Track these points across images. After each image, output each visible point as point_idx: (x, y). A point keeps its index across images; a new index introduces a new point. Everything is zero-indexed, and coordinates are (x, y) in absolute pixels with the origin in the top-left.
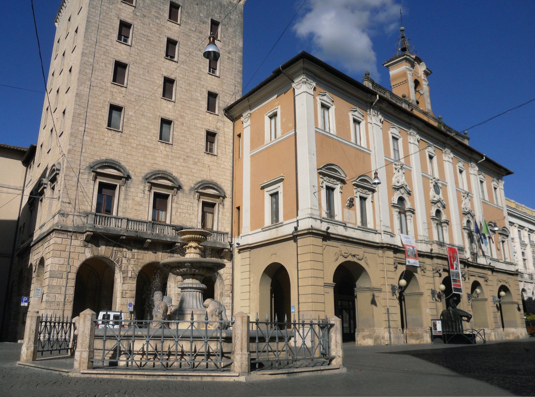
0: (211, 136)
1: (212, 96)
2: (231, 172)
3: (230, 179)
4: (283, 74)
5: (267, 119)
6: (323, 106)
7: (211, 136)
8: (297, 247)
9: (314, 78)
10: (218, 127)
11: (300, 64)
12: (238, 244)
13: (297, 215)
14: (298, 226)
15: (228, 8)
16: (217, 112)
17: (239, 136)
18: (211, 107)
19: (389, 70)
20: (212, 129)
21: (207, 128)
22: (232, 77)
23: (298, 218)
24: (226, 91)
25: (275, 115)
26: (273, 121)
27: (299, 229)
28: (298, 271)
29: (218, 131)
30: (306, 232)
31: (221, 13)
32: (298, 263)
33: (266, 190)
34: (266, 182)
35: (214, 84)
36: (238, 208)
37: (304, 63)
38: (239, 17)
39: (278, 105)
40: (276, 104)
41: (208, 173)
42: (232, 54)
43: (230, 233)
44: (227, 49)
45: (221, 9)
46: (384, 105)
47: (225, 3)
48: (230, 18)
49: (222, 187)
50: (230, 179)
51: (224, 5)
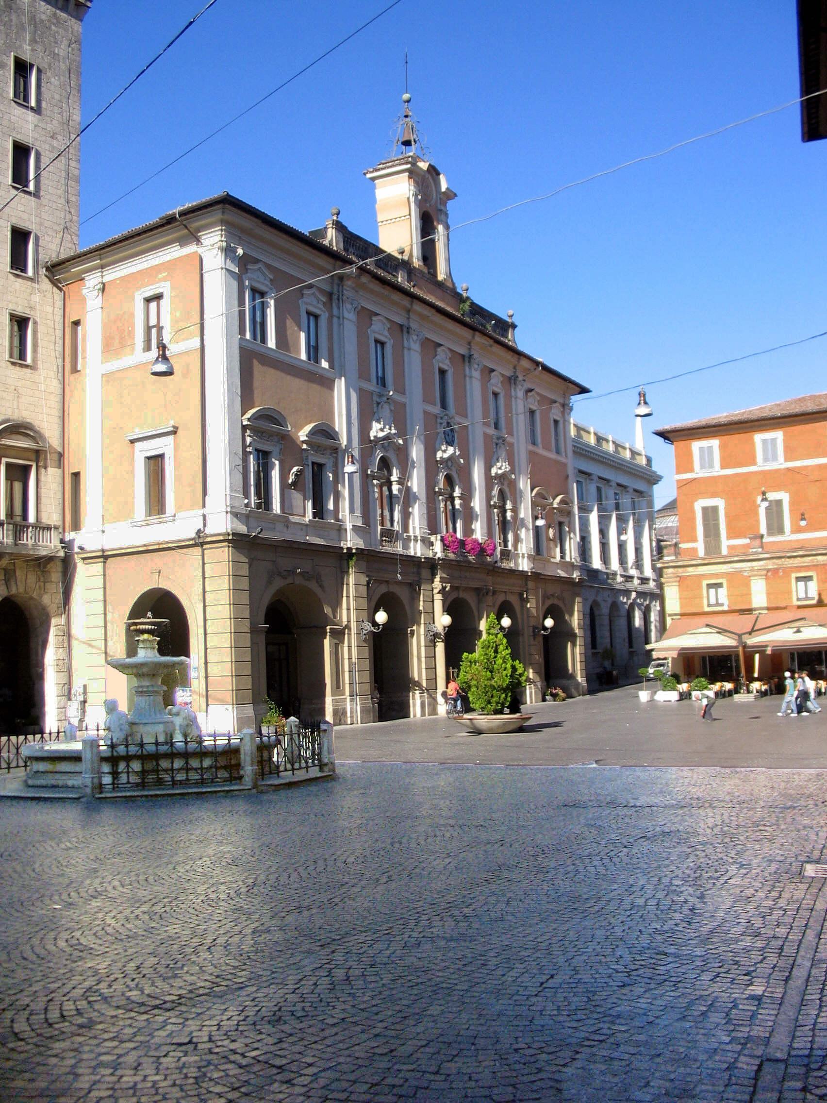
0: (20, 323)
1: (20, 237)
2: (59, 398)
3: (56, 413)
4: (178, 223)
5: (140, 305)
6: (254, 291)
7: (20, 323)
8: (204, 564)
9: (240, 238)
10: (32, 303)
11: (217, 214)
12: (81, 548)
13: (204, 506)
14: (205, 525)
15: (49, 28)
16: (30, 272)
17: (77, 323)
18: (18, 262)
19: (374, 188)
20: (20, 310)
21: (11, 306)
22: (59, 192)
23: (206, 511)
24: (47, 224)
25: (158, 297)
26: (153, 305)
27: (208, 531)
28: (205, 606)
29: (32, 313)
30: (221, 538)
31: (36, 42)
32: (204, 592)
33: (137, 444)
34: (138, 433)
35: (22, 209)
36: (76, 475)
37: (223, 212)
38: (73, 50)
39: (164, 280)
40: (160, 276)
41: (15, 403)
42: (60, 137)
43: (60, 523)
44: (49, 127)
45: (35, 32)
46: (365, 279)
47: (44, 17)
48: (55, 54)
49: (42, 431)
50: (57, 414)
51: (42, 21)
